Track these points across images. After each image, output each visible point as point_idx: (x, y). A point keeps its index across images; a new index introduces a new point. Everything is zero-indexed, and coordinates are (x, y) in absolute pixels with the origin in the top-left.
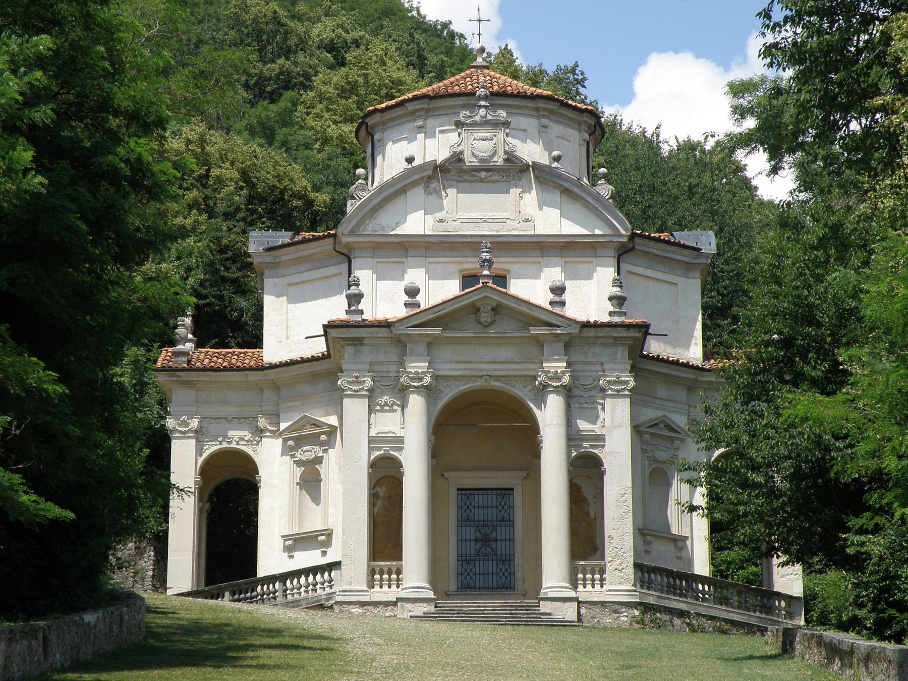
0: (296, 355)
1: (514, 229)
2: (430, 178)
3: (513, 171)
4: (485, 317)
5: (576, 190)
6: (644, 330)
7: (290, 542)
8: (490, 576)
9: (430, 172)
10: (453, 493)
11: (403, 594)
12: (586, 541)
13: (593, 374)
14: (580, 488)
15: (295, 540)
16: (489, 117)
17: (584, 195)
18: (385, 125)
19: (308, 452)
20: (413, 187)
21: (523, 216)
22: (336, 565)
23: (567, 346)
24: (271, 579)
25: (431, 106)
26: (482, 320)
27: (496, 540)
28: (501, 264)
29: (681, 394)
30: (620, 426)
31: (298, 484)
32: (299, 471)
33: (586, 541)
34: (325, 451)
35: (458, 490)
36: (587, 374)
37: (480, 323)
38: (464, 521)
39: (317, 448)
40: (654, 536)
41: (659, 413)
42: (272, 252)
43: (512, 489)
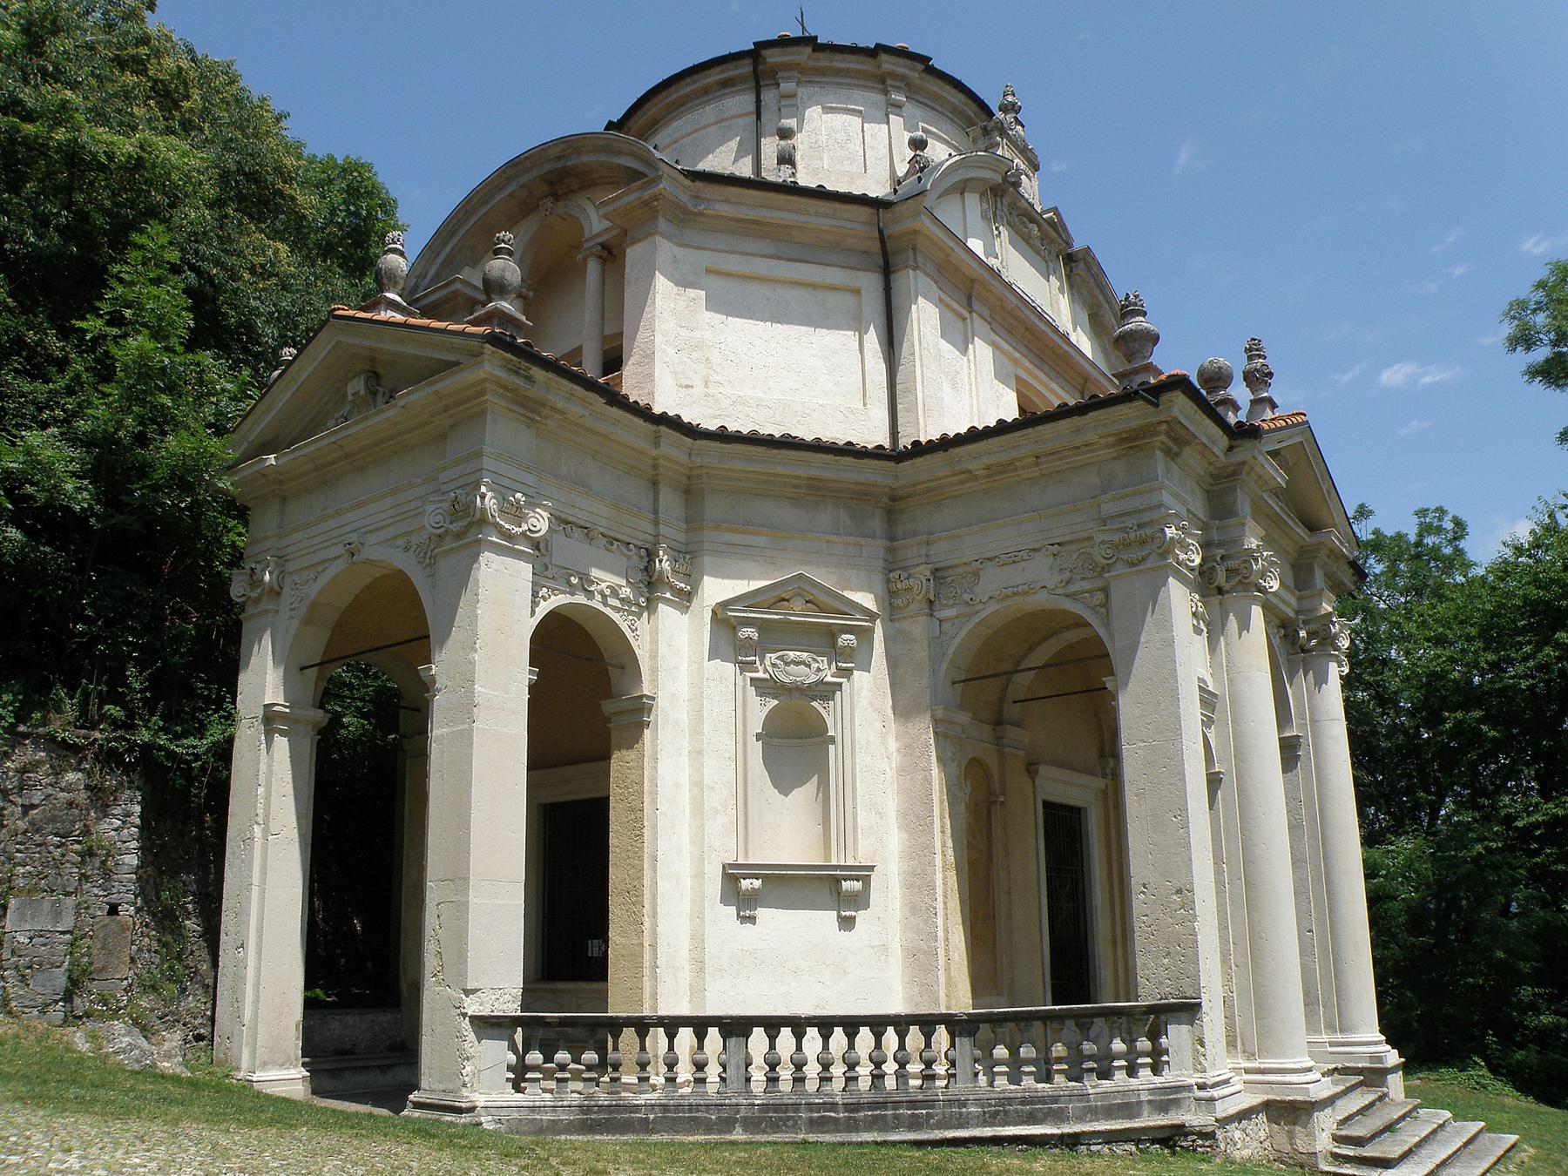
7: (757, 883)
18: (809, 75)
31: (759, 737)
32: (759, 709)
34: (847, 673)
39: (823, 662)
42: (699, 184)
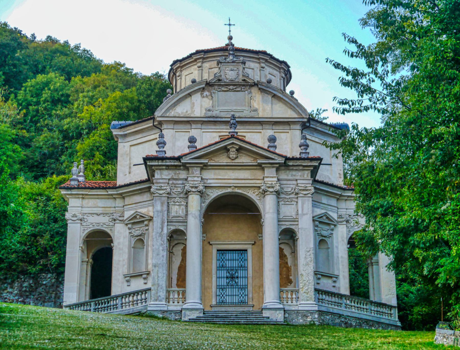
0: (133, 181)
1: (246, 113)
2: (203, 88)
3: (246, 84)
4: (233, 154)
5: (280, 95)
6: (319, 161)
8: (234, 297)
9: (204, 86)
10: (215, 252)
11: (185, 306)
12: (286, 277)
13: (292, 186)
14: (283, 249)
15: (131, 277)
16: (235, 59)
17: (284, 98)
19: (138, 230)
20: (195, 93)
21: (252, 109)
22: (150, 289)
23: (278, 170)
24: (117, 297)
25: (205, 56)
26: (231, 156)
27: (237, 277)
28: (241, 131)
29: (333, 202)
30: (307, 214)
32: (133, 240)
33: (286, 277)
35: (218, 250)
36: (288, 186)
37: (230, 158)
38: (221, 268)
40: (322, 275)
41: (323, 211)
43: (246, 250)
